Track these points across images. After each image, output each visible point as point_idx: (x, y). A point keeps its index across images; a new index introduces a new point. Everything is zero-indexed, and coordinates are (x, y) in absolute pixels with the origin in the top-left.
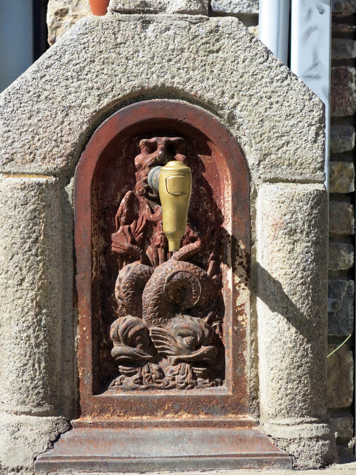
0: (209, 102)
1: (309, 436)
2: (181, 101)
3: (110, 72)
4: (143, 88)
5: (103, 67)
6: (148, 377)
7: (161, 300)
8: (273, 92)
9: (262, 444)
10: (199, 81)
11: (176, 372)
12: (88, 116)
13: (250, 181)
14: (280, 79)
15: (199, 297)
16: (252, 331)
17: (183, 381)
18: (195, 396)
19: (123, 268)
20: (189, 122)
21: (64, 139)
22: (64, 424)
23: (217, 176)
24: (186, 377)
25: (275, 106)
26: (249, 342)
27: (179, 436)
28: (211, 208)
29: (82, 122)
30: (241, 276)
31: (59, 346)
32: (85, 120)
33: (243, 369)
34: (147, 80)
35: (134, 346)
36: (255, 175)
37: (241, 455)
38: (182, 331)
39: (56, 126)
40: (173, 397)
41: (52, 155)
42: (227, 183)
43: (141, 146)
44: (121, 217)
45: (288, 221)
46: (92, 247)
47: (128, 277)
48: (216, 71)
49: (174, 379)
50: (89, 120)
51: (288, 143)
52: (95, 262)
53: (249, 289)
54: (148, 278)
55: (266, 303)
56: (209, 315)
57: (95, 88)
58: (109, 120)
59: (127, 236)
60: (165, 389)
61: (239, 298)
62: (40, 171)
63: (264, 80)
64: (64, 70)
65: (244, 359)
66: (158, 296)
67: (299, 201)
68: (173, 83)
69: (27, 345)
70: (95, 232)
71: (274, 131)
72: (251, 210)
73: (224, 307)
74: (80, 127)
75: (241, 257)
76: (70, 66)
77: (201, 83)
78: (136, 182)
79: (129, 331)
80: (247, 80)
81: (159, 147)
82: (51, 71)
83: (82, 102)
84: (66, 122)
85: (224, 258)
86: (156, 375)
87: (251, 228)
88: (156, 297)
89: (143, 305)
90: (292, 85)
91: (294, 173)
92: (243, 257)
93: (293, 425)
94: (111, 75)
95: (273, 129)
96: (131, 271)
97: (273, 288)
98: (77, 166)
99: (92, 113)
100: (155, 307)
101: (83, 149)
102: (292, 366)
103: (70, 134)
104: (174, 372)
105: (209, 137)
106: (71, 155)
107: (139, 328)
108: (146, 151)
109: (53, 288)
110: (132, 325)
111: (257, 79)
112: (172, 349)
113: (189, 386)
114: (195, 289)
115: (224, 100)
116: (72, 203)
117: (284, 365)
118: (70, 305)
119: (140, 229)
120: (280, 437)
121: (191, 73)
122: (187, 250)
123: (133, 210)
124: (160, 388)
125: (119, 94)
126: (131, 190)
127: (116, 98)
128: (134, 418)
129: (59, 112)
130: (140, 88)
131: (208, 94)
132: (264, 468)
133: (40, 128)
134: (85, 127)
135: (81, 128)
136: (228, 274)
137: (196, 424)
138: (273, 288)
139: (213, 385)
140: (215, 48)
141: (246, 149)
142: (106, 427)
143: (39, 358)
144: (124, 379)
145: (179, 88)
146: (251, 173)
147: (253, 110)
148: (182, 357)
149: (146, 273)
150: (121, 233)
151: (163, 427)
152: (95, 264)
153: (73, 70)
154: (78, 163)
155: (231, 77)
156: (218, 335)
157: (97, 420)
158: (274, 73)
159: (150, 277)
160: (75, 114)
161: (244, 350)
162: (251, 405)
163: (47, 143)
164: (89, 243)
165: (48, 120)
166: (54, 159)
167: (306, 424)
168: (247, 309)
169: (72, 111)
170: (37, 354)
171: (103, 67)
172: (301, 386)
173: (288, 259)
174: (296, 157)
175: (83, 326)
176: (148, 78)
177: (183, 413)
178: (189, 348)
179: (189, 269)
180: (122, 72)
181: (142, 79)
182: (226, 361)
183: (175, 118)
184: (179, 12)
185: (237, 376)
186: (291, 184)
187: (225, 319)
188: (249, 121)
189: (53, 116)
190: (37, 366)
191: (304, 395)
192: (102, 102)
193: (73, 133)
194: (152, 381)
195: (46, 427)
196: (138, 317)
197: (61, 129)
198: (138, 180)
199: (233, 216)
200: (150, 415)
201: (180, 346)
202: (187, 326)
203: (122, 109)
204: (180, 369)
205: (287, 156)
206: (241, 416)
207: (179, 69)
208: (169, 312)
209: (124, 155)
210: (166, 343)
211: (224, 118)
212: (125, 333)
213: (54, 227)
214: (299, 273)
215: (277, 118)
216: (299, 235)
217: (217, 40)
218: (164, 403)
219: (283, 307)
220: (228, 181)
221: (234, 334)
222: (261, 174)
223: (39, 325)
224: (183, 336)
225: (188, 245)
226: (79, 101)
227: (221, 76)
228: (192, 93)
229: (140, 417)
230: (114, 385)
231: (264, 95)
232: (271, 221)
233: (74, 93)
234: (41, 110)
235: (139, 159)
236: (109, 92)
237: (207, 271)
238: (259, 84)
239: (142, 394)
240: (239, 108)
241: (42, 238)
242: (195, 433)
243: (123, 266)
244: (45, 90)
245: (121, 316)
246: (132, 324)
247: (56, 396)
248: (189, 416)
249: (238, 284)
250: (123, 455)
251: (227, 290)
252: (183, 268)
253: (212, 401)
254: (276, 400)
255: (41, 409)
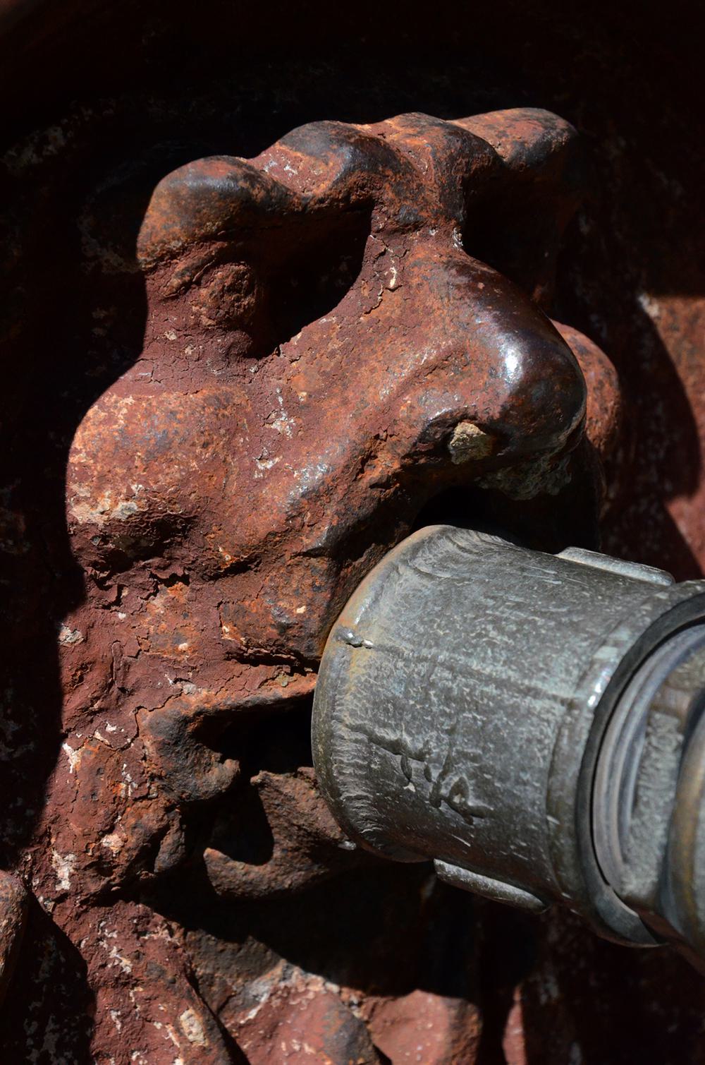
78: (53, 757)
108: (228, 324)
198: (89, 715)
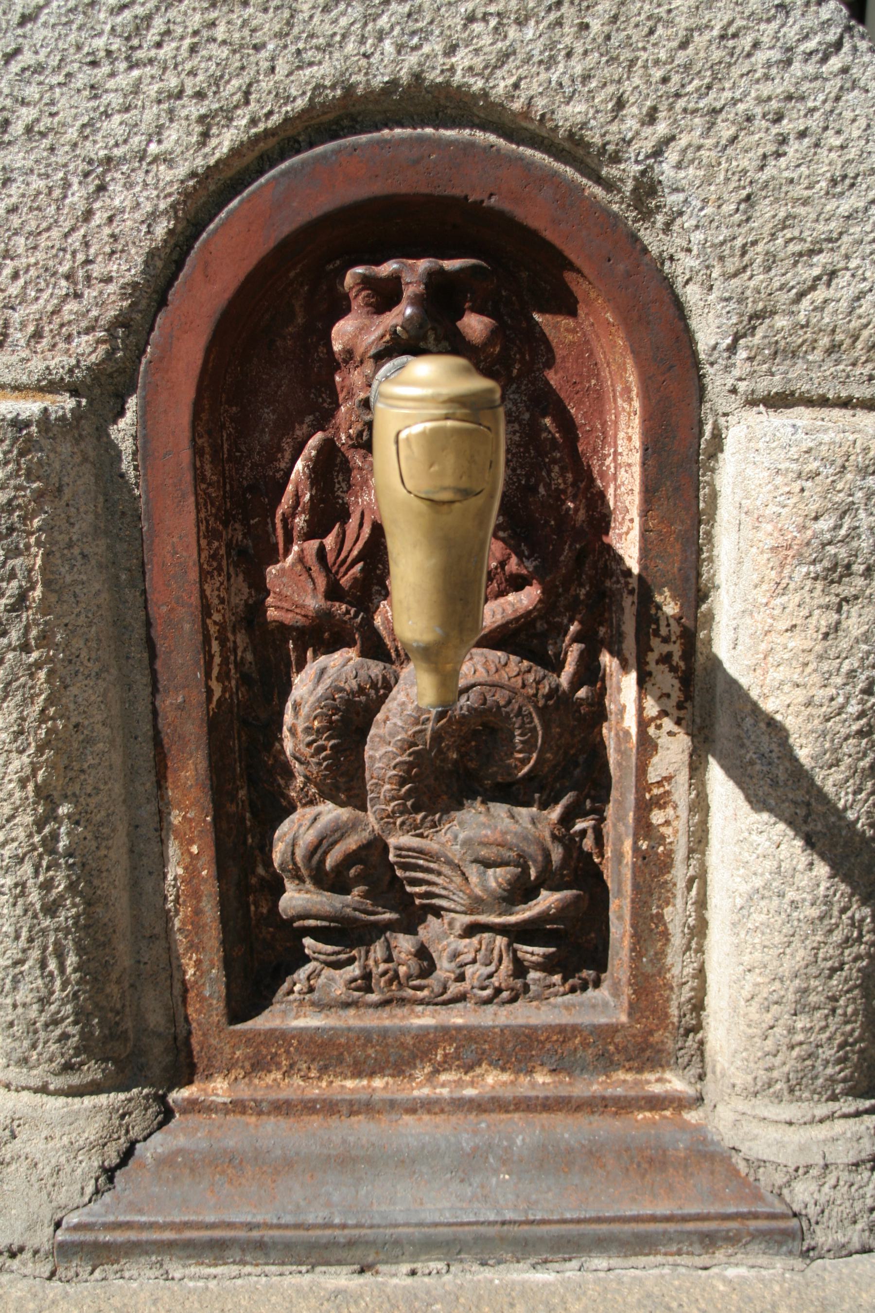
0: (571, 135)
1: (851, 1158)
2: (480, 136)
3: (237, 35)
4: (349, 90)
5: (213, 15)
6: (385, 973)
7: (418, 766)
8: (789, 98)
9: (712, 1173)
10: (541, 62)
11: (469, 957)
12: (169, 190)
13: (701, 399)
14: (817, 51)
15: (535, 756)
16: (691, 851)
17: (487, 982)
18: (521, 1026)
19: (307, 667)
20: (507, 206)
21: (96, 270)
22: (146, 1109)
23: (593, 382)
24: (496, 971)
25: (793, 148)
26: (681, 884)
27: (476, 1149)
28: (574, 484)
29: (153, 213)
30: (662, 697)
31: (120, 899)
32: (162, 206)
33: (661, 954)
34: (363, 62)
35: (348, 893)
37: (653, 1219)
38: (484, 852)
39: (67, 226)
40: (458, 1029)
41: (62, 325)
42: (626, 406)
43: (351, 289)
44: (293, 515)
45: (828, 536)
46: (206, 610)
47: (319, 700)
48: (596, 26)
49: (461, 978)
50: (173, 206)
51: (833, 274)
52: (217, 654)
53: (687, 734)
54: (381, 700)
55: (740, 784)
56: (564, 801)
57: (189, 91)
58: (241, 203)
59: (314, 575)
60: (436, 1004)
61: (655, 760)
62: (24, 379)
63: (761, 57)
64: (80, 28)
65: (666, 929)
66: (410, 755)
68: (452, 69)
69: (19, 911)
70: (215, 564)
71: (789, 236)
72: (702, 493)
73: (609, 777)
74: (144, 228)
75: (666, 640)
76: (102, 16)
77: (548, 69)
79: (326, 853)
80: (702, 55)
81: (409, 292)
82: (39, 32)
83: (149, 141)
84: (98, 214)
85: (612, 637)
86: (409, 967)
87: (699, 551)
88: (405, 758)
89: (367, 775)
90: (855, 71)
91: (848, 377)
92: (673, 638)
93: (805, 1123)
94: (242, 46)
95: (783, 228)
96: (327, 682)
97: (766, 743)
98: (144, 361)
99: (182, 182)
100: (402, 784)
101: (162, 302)
102: (813, 970)
103: (113, 252)
104: (462, 957)
105: (572, 257)
106: (122, 321)
107: (356, 841)
108: (367, 305)
109: (89, 741)
110: (337, 835)
111: (738, 51)
112: (455, 897)
113: (505, 995)
114: (521, 735)
115: (623, 127)
116: (136, 477)
117: (788, 966)
118: (147, 782)
119: (355, 553)
120: (765, 1158)
121: (513, 32)
122: (499, 616)
123: (333, 492)
124: (422, 1002)
125: (270, 113)
126: (324, 430)
127: (261, 127)
128: (349, 1084)
129: (75, 180)
130: (339, 92)
131: (569, 109)
132: (720, 1255)
133: (16, 234)
134: (161, 229)
135: (149, 232)
136: (623, 685)
137: (523, 1106)
138: (766, 743)
139: (573, 990)
141: (692, 294)
142: (269, 1114)
143: (57, 943)
144: (319, 975)
145: (470, 86)
146: (704, 376)
147: (719, 164)
148: (483, 919)
149: (374, 685)
150: (293, 565)
151: (429, 1112)
152: (217, 660)
153: (113, 29)
154: (149, 349)
155: (649, 46)
156: (590, 855)
157: (244, 1092)
158: (797, 27)
159: (386, 696)
160: (129, 185)
161: (668, 904)
162: (681, 1049)
163: (43, 285)
164: (195, 600)
165: (39, 209)
166: (69, 339)
167: (842, 1121)
168: (681, 793)
169: (118, 175)
170: (52, 933)
171: (213, 15)
172: (834, 1022)
173: (821, 658)
174: (855, 324)
175: (191, 842)
176: (366, 56)
177: (487, 1071)
178: (504, 899)
179: (504, 676)
180: (279, 35)
181: (347, 58)
182: (612, 929)
183: (457, 192)
185: (643, 974)
186: (836, 413)
187: (610, 810)
188: (705, 201)
189: (57, 193)
190: (52, 965)
191: (841, 1047)
192: (214, 142)
193: (123, 251)
194: (399, 983)
195: (92, 1131)
196: (356, 807)
197: (84, 236)
198: (346, 400)
199: (645, 514)
200: (393, 1076)
201: (478, 891)
202: (498, 836)
203: (283, 166)
204: (478, 951)
205: (827, 320)
206: (652, 1077)
207: (471, 19)
208: (445, 797)
209: (300, 320)
210: (439, 880)
211: (619, 191)
212: (316, 857)
213: (79, 557)
214: (853, 701)
215: (799, 191)
216: (860, 582)
218: (434, 1045)
219: (795, 803)
220: (630, 400)
221: (640, 862)
222: (740, 379)
223: (52, 851)
224: (487, 864)
225: (502, 600)
226: (136, 141)
227: (614, 42)
228: (517, 106)
229: (365, 1082)
230: (291, 992)
231: (758, 111)
232: (767, 534)
233: (119, 112)
234: (15, 175)
235: (344, 334)
236: (236, 107)
237: (559, 676)
238: (745, 71)
239: (372, 1020)
240: (672, 155)
241: (37, 593)
242: (519, 1142)
243: (305, 662)
244: (24, 103)
245: (304, 805)
246: (334, 831)
247: (123, 1037)
248: (506, 1077)
249: (653, 719)
250: (311, 1219)
251: (621, 734)
252: (485, 674)
253: (569, 1039)
254: (760, 1054)
255: (74, 1080)
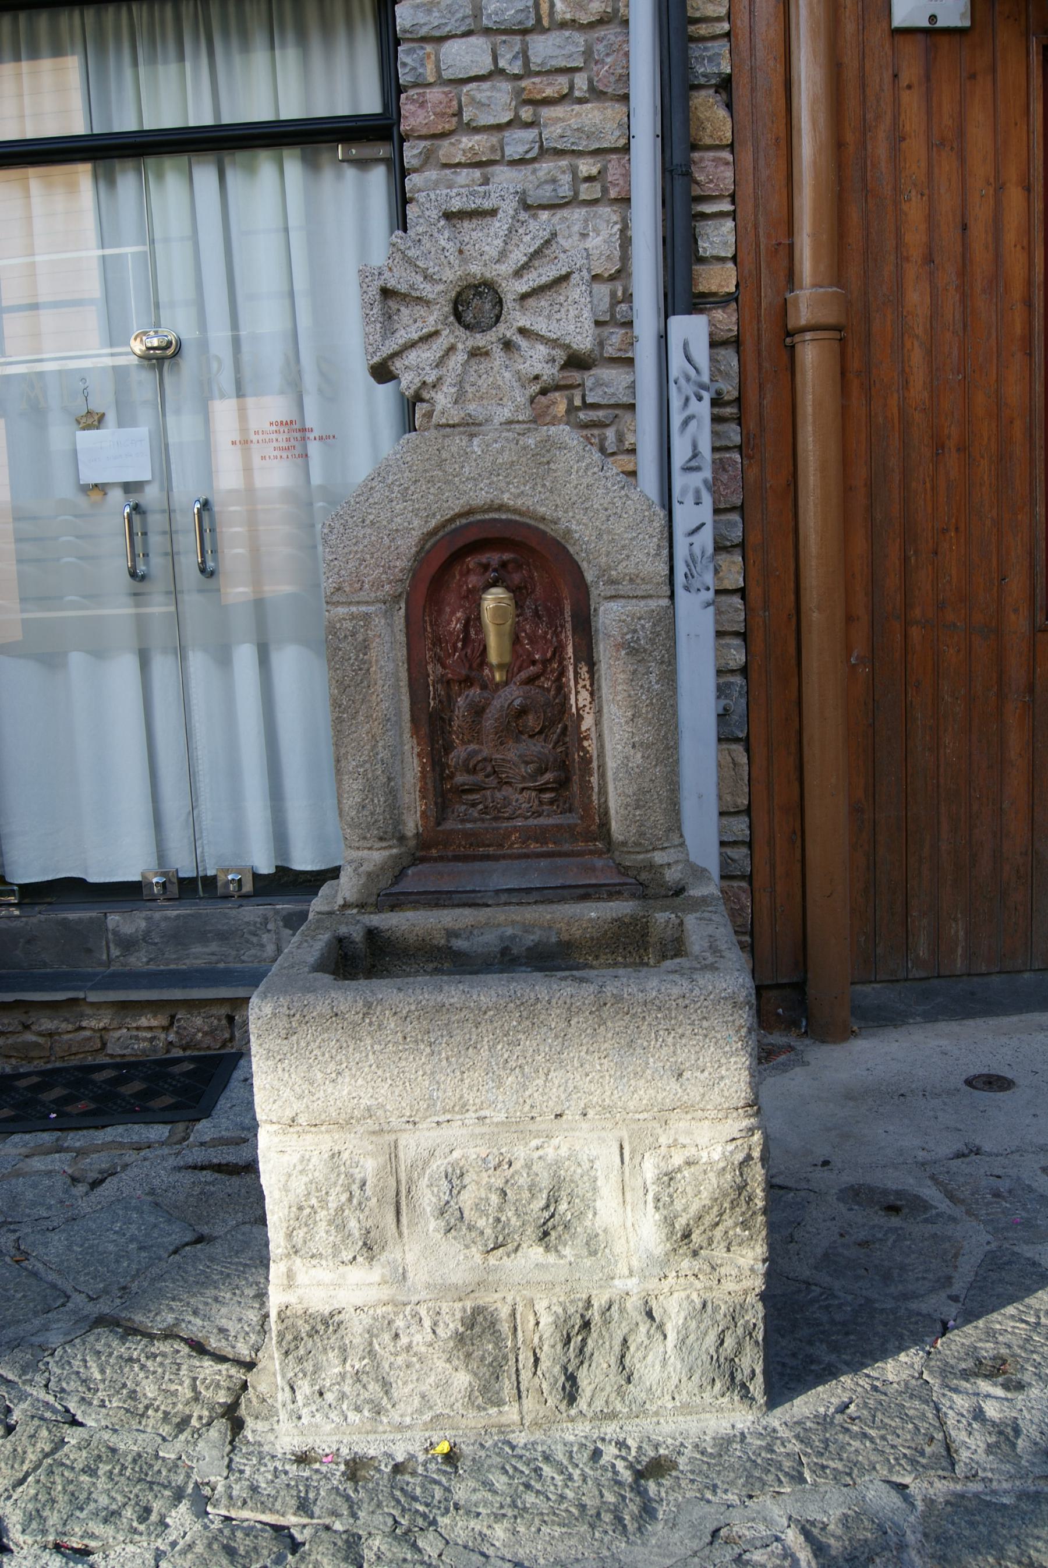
36: (594, 592)
67: (639, 619)
140: (545, 460)
148: (526, 785)
168: (593, 735)
184: (506, 423)
186: (634, 600)
217: (548, 451)
218: (511, 833)
